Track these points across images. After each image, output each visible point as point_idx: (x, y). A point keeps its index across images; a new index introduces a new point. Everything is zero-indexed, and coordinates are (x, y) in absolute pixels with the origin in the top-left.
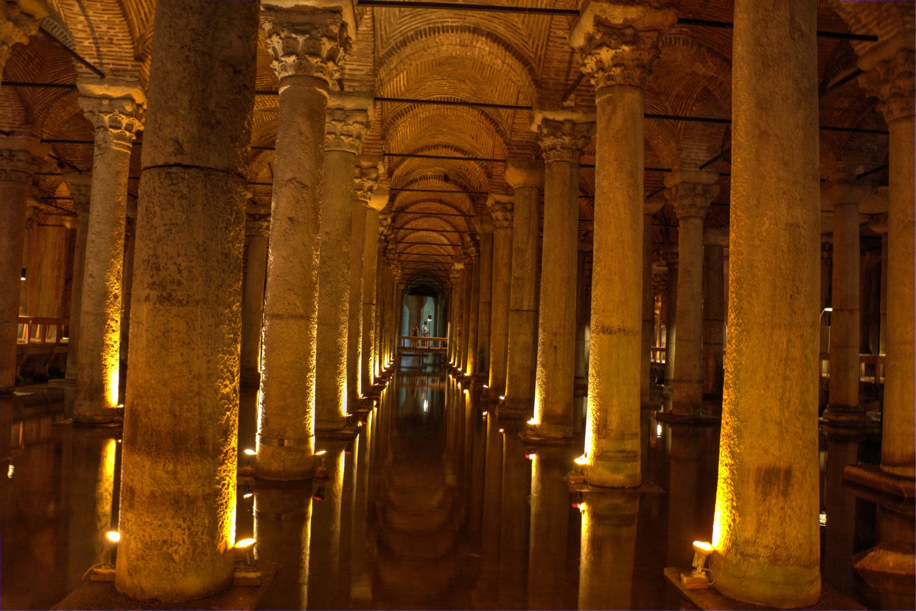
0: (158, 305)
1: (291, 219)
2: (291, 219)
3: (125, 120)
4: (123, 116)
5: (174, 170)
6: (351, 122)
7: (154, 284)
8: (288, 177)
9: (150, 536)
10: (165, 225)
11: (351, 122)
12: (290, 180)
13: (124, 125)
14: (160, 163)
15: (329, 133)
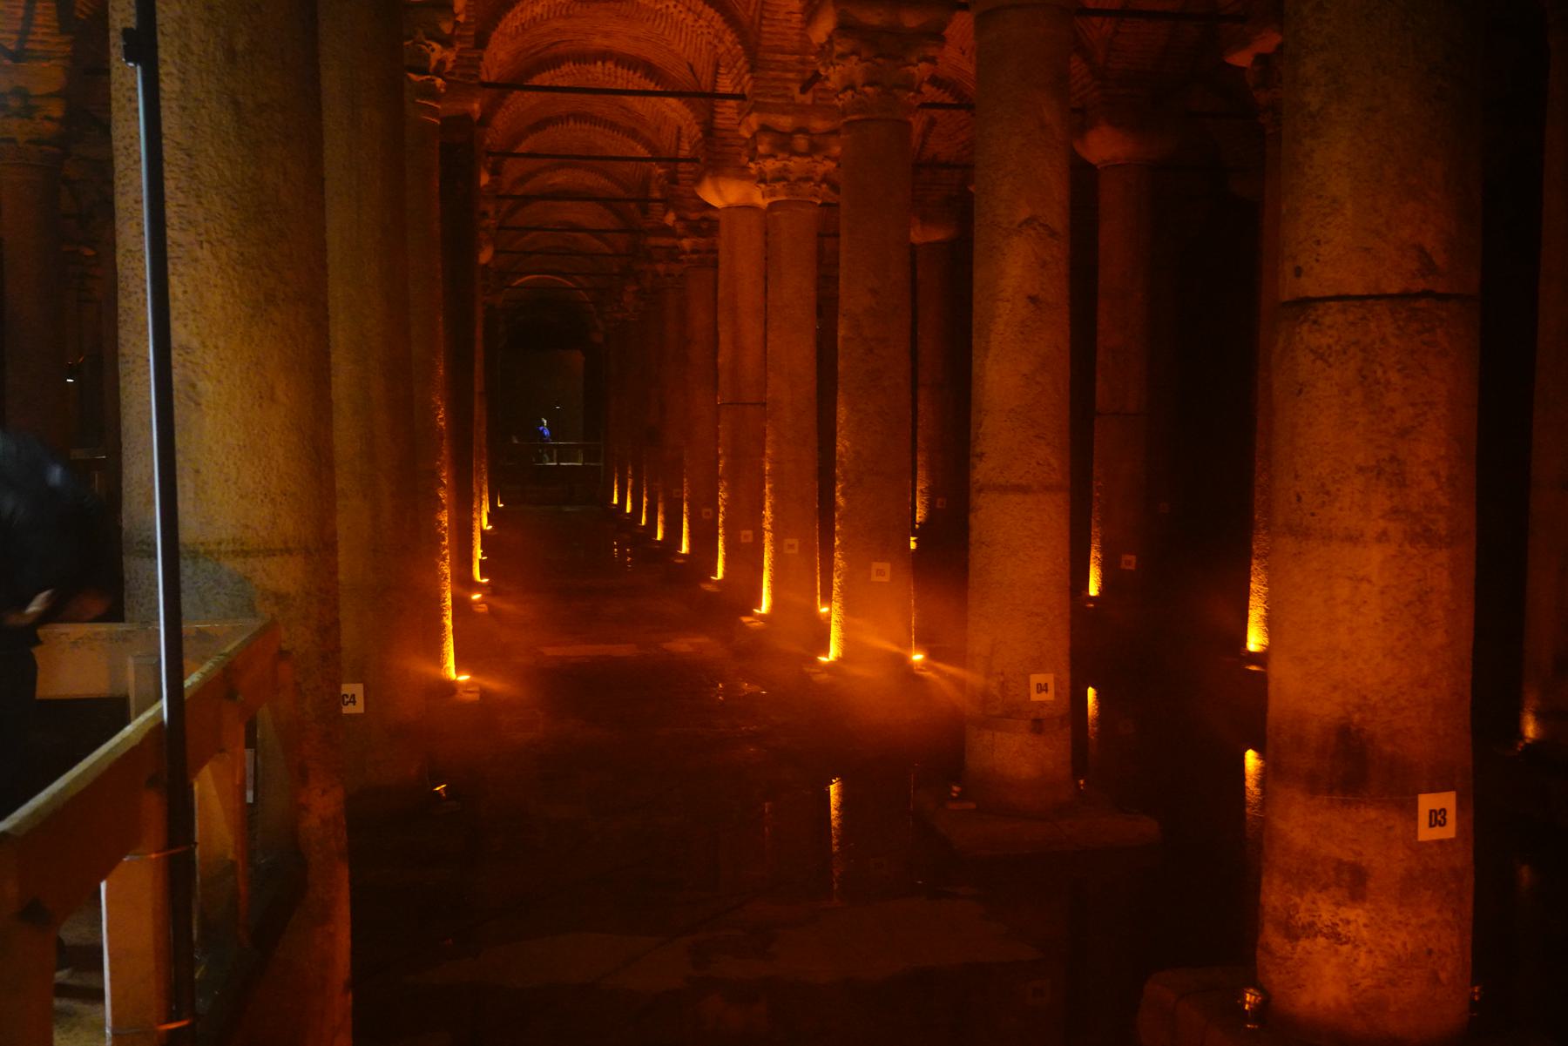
0: (1407, 547)
1: (1033, 299)
2: (1033, 299)
3: (437, 52)
4: (435, 45)
5: (1422, 303)
6: (914, 60)
7: (1395, 511)
8: (1023, 217)
9: (1404, 944)
10: (1413, 405)
11: (914, 60)
12: (1026, 222)
13: (434, 64)
14: (1394, 290)
15: (870, 84)
